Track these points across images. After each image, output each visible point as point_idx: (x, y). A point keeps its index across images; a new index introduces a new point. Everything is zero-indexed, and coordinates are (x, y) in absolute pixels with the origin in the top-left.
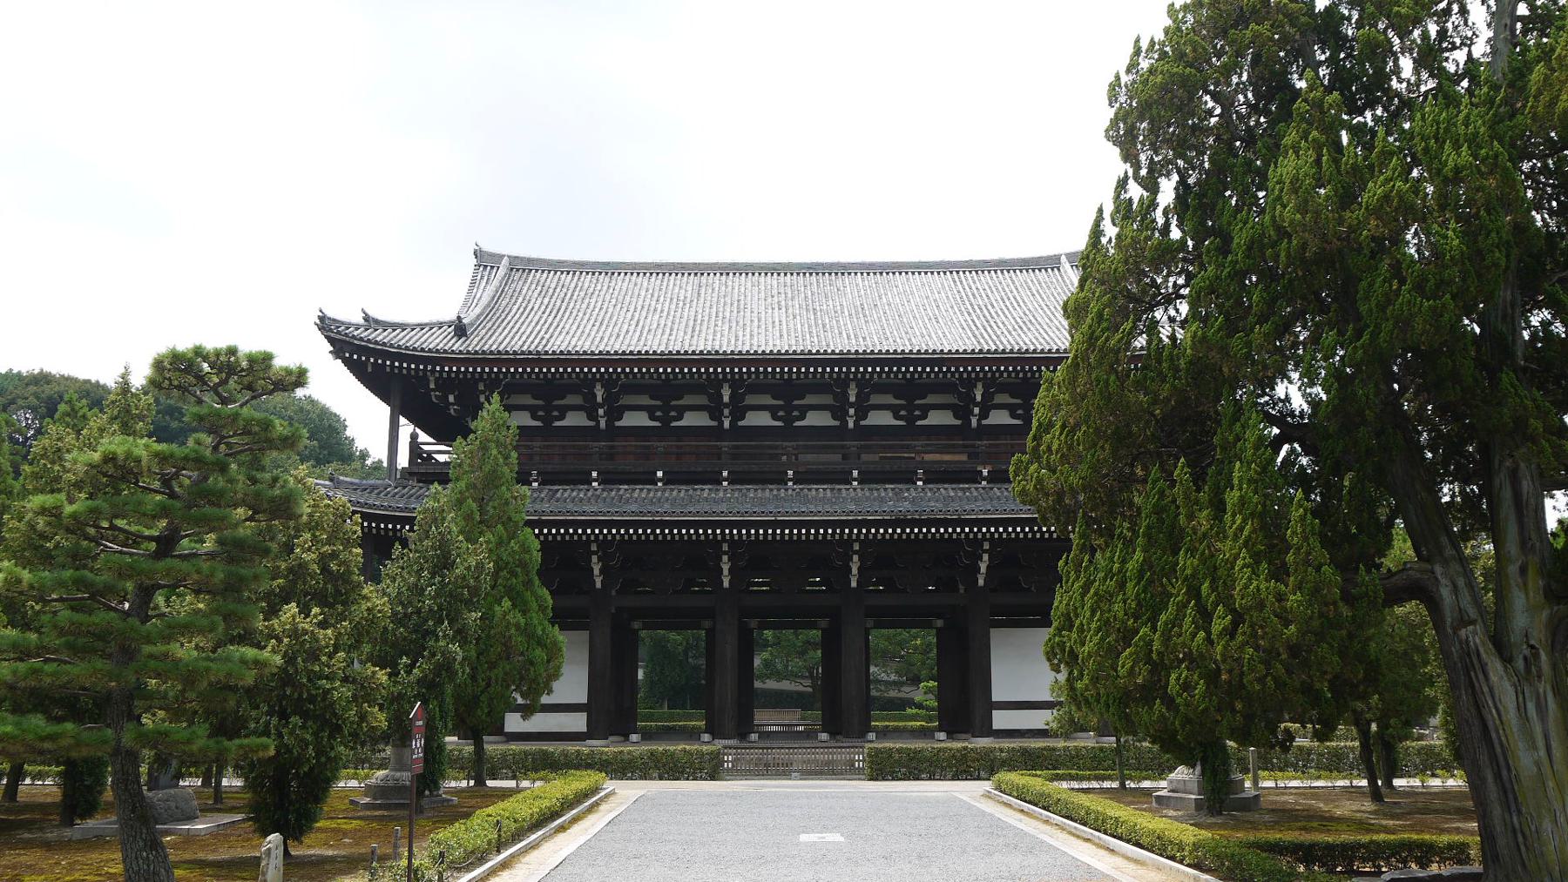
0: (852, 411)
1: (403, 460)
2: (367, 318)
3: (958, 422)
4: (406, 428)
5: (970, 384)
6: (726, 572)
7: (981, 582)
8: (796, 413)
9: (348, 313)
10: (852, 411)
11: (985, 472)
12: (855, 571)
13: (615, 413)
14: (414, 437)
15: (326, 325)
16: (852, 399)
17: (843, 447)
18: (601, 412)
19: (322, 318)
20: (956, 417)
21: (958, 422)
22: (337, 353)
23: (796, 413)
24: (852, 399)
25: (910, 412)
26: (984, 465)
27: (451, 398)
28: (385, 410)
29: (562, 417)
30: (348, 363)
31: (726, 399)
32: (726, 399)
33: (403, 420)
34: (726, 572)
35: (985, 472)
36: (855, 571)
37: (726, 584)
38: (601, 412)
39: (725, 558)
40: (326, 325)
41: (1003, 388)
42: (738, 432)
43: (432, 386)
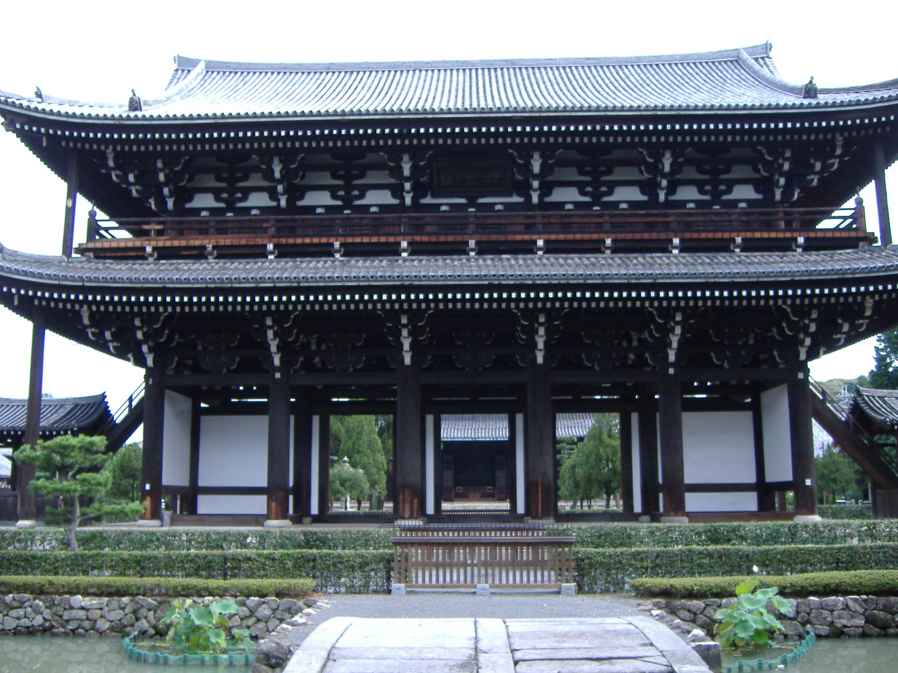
0: (536, 184)
1: (80, 237)
4: (84, 205)
6: (406, 346)
10: (536, 184)
12: (541, 345)
14: (92, 214)
16: (536, 168)
18: (280, 188)
22: (10, 125)
24: (536, 168)
28: (62, 186)
30: (21, 134)
31: (407, 172)
32: (407, 172)
33: (79, 197)
34: (406, 346)
36: (541, 345)
37: (408, 360)
38: (280, 188)
39: (405, 332)
41: (689, 162)
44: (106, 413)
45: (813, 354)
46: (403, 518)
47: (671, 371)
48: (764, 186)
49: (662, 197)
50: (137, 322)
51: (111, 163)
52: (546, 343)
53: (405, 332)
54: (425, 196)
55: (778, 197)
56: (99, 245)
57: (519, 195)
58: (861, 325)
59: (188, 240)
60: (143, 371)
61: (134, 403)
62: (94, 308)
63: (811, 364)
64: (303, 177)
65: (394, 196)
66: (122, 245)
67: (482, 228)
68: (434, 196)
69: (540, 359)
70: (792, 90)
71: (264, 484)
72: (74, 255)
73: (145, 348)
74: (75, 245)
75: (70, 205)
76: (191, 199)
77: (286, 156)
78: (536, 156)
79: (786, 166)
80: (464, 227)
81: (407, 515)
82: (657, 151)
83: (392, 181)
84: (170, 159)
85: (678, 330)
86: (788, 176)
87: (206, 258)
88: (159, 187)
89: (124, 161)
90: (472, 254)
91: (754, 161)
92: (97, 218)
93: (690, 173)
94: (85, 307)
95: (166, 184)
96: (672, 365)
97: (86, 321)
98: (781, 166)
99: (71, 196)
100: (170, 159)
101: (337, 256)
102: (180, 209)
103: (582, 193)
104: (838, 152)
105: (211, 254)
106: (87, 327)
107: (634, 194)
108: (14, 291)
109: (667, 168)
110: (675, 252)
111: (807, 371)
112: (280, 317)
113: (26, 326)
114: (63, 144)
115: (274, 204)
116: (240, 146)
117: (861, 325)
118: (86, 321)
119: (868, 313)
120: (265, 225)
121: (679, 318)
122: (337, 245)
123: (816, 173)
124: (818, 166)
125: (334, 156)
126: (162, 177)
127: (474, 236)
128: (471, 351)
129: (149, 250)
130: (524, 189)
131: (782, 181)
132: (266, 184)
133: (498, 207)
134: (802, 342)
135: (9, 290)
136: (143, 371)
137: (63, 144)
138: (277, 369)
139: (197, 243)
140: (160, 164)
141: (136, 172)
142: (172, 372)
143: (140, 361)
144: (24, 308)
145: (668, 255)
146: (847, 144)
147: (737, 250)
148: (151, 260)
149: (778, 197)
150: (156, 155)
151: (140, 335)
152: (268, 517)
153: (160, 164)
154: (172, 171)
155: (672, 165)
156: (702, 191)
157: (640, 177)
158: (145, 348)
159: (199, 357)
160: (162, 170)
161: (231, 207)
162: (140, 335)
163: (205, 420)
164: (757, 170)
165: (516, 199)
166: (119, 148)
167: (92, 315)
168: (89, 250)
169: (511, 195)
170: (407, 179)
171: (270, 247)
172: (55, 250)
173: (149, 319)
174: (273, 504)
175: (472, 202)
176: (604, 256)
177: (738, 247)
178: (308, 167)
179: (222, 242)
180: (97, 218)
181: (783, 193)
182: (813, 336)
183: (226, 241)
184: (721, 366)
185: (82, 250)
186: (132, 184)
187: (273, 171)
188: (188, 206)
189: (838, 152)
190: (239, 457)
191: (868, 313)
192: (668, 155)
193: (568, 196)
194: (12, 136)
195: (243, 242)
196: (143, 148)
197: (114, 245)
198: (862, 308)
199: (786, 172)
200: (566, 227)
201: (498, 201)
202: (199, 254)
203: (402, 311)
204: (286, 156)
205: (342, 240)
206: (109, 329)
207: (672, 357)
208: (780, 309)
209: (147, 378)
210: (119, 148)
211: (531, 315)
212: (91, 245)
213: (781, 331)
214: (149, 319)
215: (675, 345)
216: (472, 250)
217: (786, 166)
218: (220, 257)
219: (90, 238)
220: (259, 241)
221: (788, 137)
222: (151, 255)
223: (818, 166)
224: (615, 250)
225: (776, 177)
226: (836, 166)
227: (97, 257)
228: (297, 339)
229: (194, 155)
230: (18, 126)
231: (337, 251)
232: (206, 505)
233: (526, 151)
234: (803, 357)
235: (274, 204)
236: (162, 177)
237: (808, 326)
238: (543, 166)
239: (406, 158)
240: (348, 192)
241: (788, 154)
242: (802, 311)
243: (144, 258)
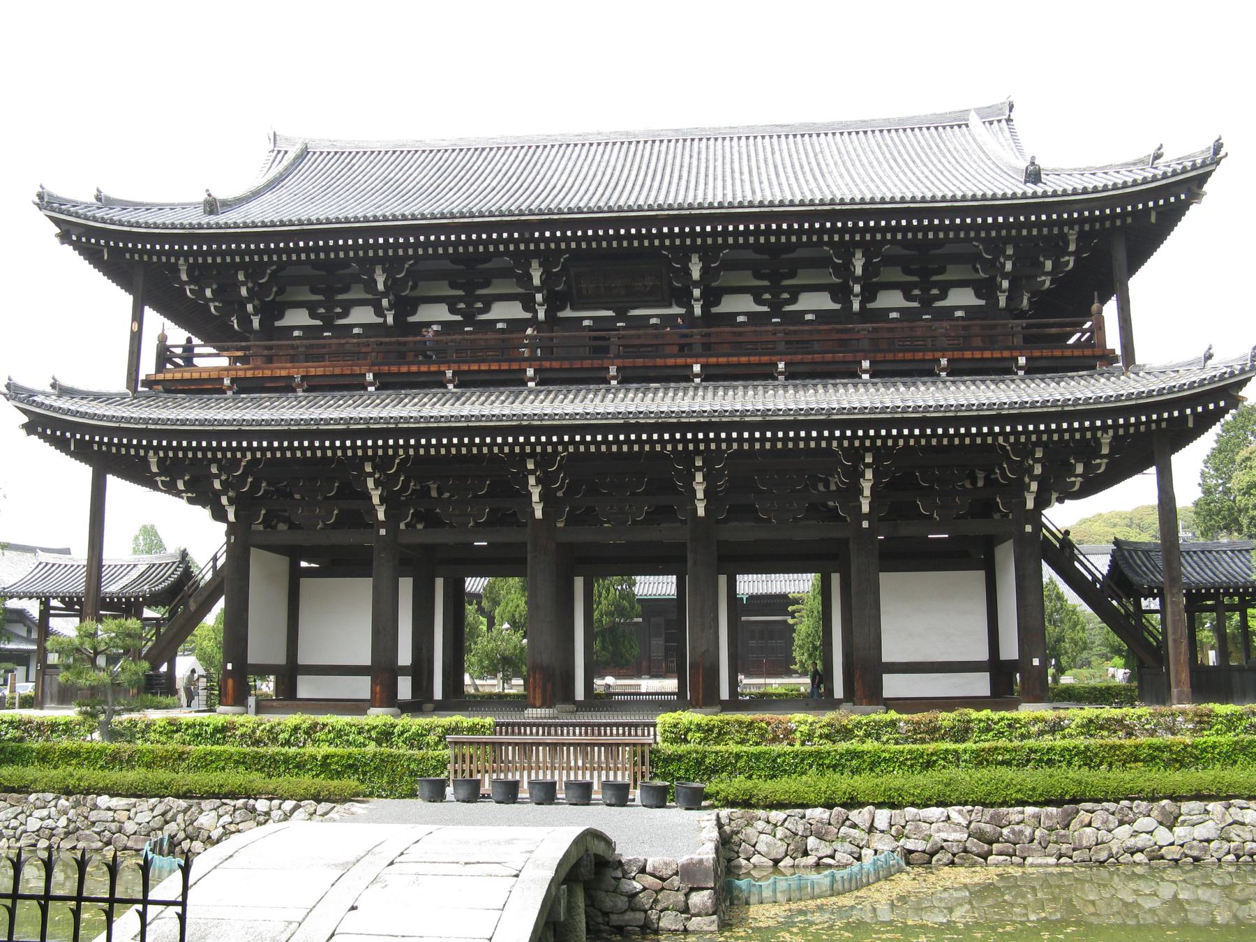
0: (697, 292)
1: (148, 366)
2: (98, 198)
3: (838, 306)
9: (78, 190)
13: (405, 306)
14: (163, 339)
15: (46, 202)
16: (696, 275)
19: (41, 196)
20: (834, 300)
21: (838, 306)
22: (65, 237)
25: (776, 295)
27: (208, 293)
30: (78, 246)
31: (537, 281)
37: (539, 514)
40: (46, 202)
41: (889, 261)
44: (187, 574)
46: (534, 706)
47: (865, 524)
48: (985, 289)
49: (856, 306)
50: (214, 470)
51: (184, 277)
52: (705, 492)
53: (532, 480)
54: (563, 309)
55: (1002, 302)
56: (169, 376)
57: (680, 305)
58: (1100, 465)
59: (272, 369)
60: (224, 526)
61: (220, 563)
62: (161, 454)
64: (414, 288)
65: (526, 309)
66: (205, 376)
67: (632, 350)
68: (573, 309)
71: (367, 661)
72: (140, 389)
73: (224, 500)
74: (142, 377)
75: (136, 329)
76: (281, 317)
77: (391, 264)
78: (695, 258)
80: (605, 350)
81: (538, 704)
82: (846, 250)
83: (521, 291)
84: (254, 271)
85: (869, 474)
86: (1014, 278)
87: (294, 390)
88: (242, 303)
89: (200, 274)
90: (614, 382)
91: (972, 259)
92: (168, 343)
94: (151, 453)
95: (250, 299)
96: (866, 516)
97: (154, 469)
98: (1003, 265)
99: (138, 317)
100: (254, 271)
101: (451, 386)
102: (269, 331)
103: (758, 301)
104: (1072, 248)
105: (300, 386)
106: (156, 474)
107: (823, 302)
108: (68, 435)
109: (859, 271)
110: (866, 377)
111: (1039, 525)
112: (382, 464)
113: (84, 472)
114: (128, 256)
115: (380, 320)
116: (332, 255)
117: (1100, 465)
118: (154, 469)
119: (1105, 451)
120: (364, 350)
121: (869, 460)
122: (449, 374)
123: (1047, 274)
124: (1049, 265)
125: (453, 262)
126: (244, 292)
127: (616, 361)
128: (619, 501)
129: (227, 382)
130: (683, 297)
131: (1005, 284)
132: (370, 296)
133: (653, 321)
134: (1028, 488)
135: (63, 434)
136: (224, 526)
137: (128, 256)
138: (382, 524)
139: (284, 373)
140: (241, 277)
141: (214, 287)
142: (261, 528)
143: (219, 515)
144: (82, 452)
145: (857, 380)
146: (1082, 236)
147: (943, 374)
148: (230, 393)
149: (1002, 302)
150: (237, 267)
151: (217, 485)
152: (373, 702)
153: (241, 277)
154: (255, 283)
155: (865, 268)
156: (908, 297)
157: (975, 276)
158: (224, 500)
159: (294, 508)
160: (243, 283)
161: (328, 324)
162: (217, 485)
163: (305, 583)
165: (676, 310)
166: (191, 260)
167: (161, 462)
168: (157, 382)
169: (670, 306)
170: (538, 290)
171: (370, 377)
172: (117, 383)
173: (228, 466)
174: (378, 689)
175: (621, 315)
176: (776, 383)
177: (943, 370)
178: (416, 276)
179: (312, 372)
180: (168, 343)
182: (1042, 480)
183: (316, 370)
184: (930, 517)
185: (149, 383)
186: (211, 300)
187: (376, 283)
188: (278, 324)
189: (1072, 248)
190: (342, 627)
191: (1105, 451)
192: (859, 254)
193: (740, 305)
194: (68, 249)
195: (337, 371)
196: (219, 260)
197: (196, 376)
198: (1099, 445)
199: (1008, 273)
200: (738, 346)
201: (653, 313)
202: (284, 387)
203: (365, 458)
204: (391, 264)
205: (456, 367)
206: (182, 478)
207: (865, 508)
209: (228, 534)
210: (191, 260)
212: (160, 377)
214: (228, 466)
215: (867, 492)
216: (614, 378)
217: (1009, 266)
218: (310, 389)
219: (160, 367)
220: (357, 370)
221: (1004, 232)
222: (230, 388)
226: (1071, 264)
227: (167, 391)
228: (405, 487)
229: (281, 266)
230: (74, 238)
231: (450, 381)
232: (307, 688)
233: (684, 254)
234: (1030, 504)
235: (380, 320)
236: (244, 292)
237: (1032, 467)
238: (704, 271)
239: (535, 264)
240: (470, 305)
241: (1010, 251)
243: (222, 391)
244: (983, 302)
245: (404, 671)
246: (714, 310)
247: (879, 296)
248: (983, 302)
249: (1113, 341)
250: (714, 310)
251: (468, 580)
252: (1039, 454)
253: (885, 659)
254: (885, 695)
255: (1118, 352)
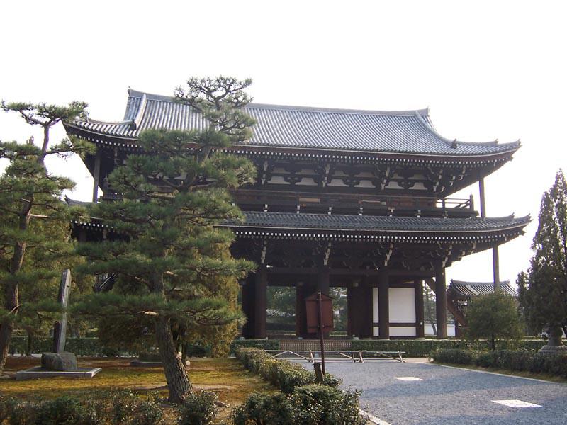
0: (326, 178)
5: (383, 167)
7: (386, 264)
8: (296, 179)
11: (392, 211)
17: (320, 195)
23: (296, 179)
26: (392, 207)
29: (299, 181)
35: (392, 211)
42: (268, 186)
43: (116, 155)
45: (449, 264)
63: (447, 269)
69: (325, 263)
70: (447, 142)
79: (440, 177)
93: (396, 176)
104: (464, 172)
124: (454, 178)
131: (438, 184)
146: (467, 169)
164: (425, 176)
181: (437, 189)
208: (436, 244)
211: (260, 240)
213: (434, 253)
217: (440, 177)
223: (454, 178)
224: (395, 214)
225: (435, 181)
234: (444, 266)
242: (445, 246)
244: (426, 189)
245: (376, 325)
246: (329, 185)
247: (332, 181)
248: (426, 189)
249: (477, 208)
250: (329, 185)
251: (377, 288)
252: (451, 248)
253: (390, 322)
254: (390, 335)
255: (479, 212)
